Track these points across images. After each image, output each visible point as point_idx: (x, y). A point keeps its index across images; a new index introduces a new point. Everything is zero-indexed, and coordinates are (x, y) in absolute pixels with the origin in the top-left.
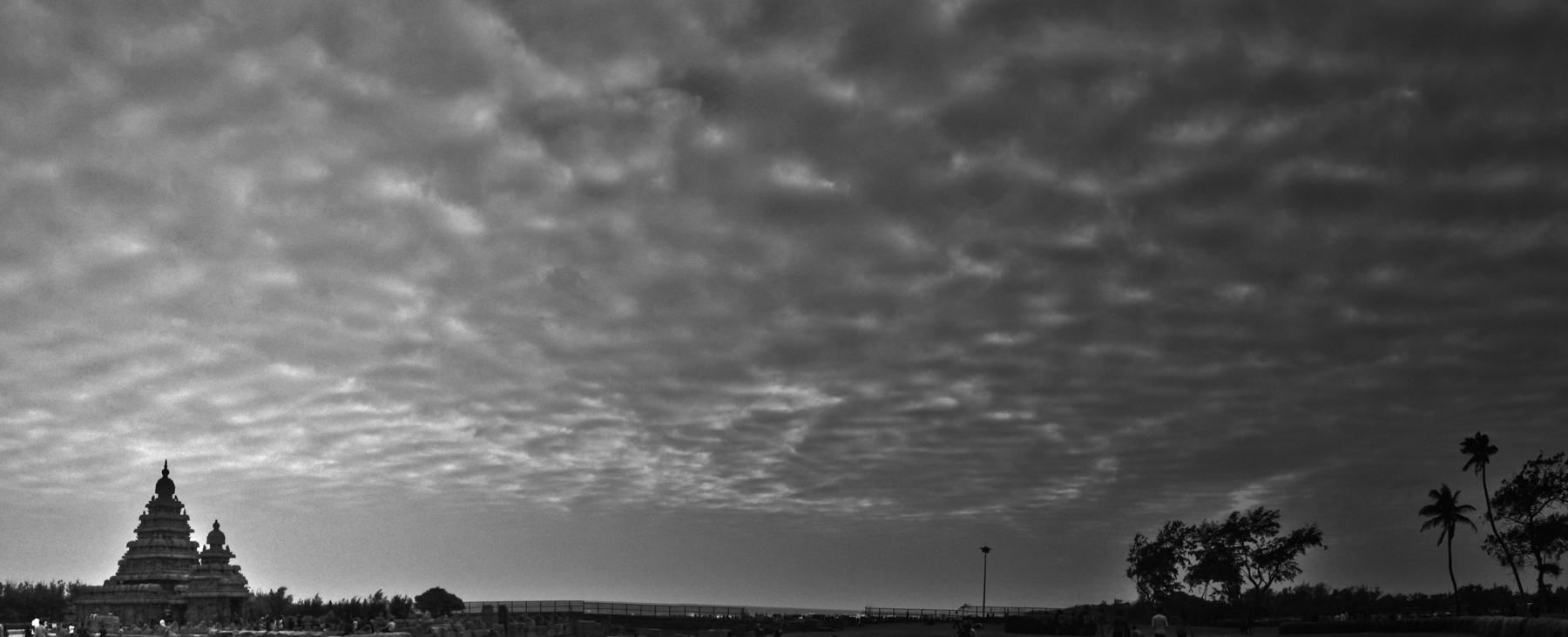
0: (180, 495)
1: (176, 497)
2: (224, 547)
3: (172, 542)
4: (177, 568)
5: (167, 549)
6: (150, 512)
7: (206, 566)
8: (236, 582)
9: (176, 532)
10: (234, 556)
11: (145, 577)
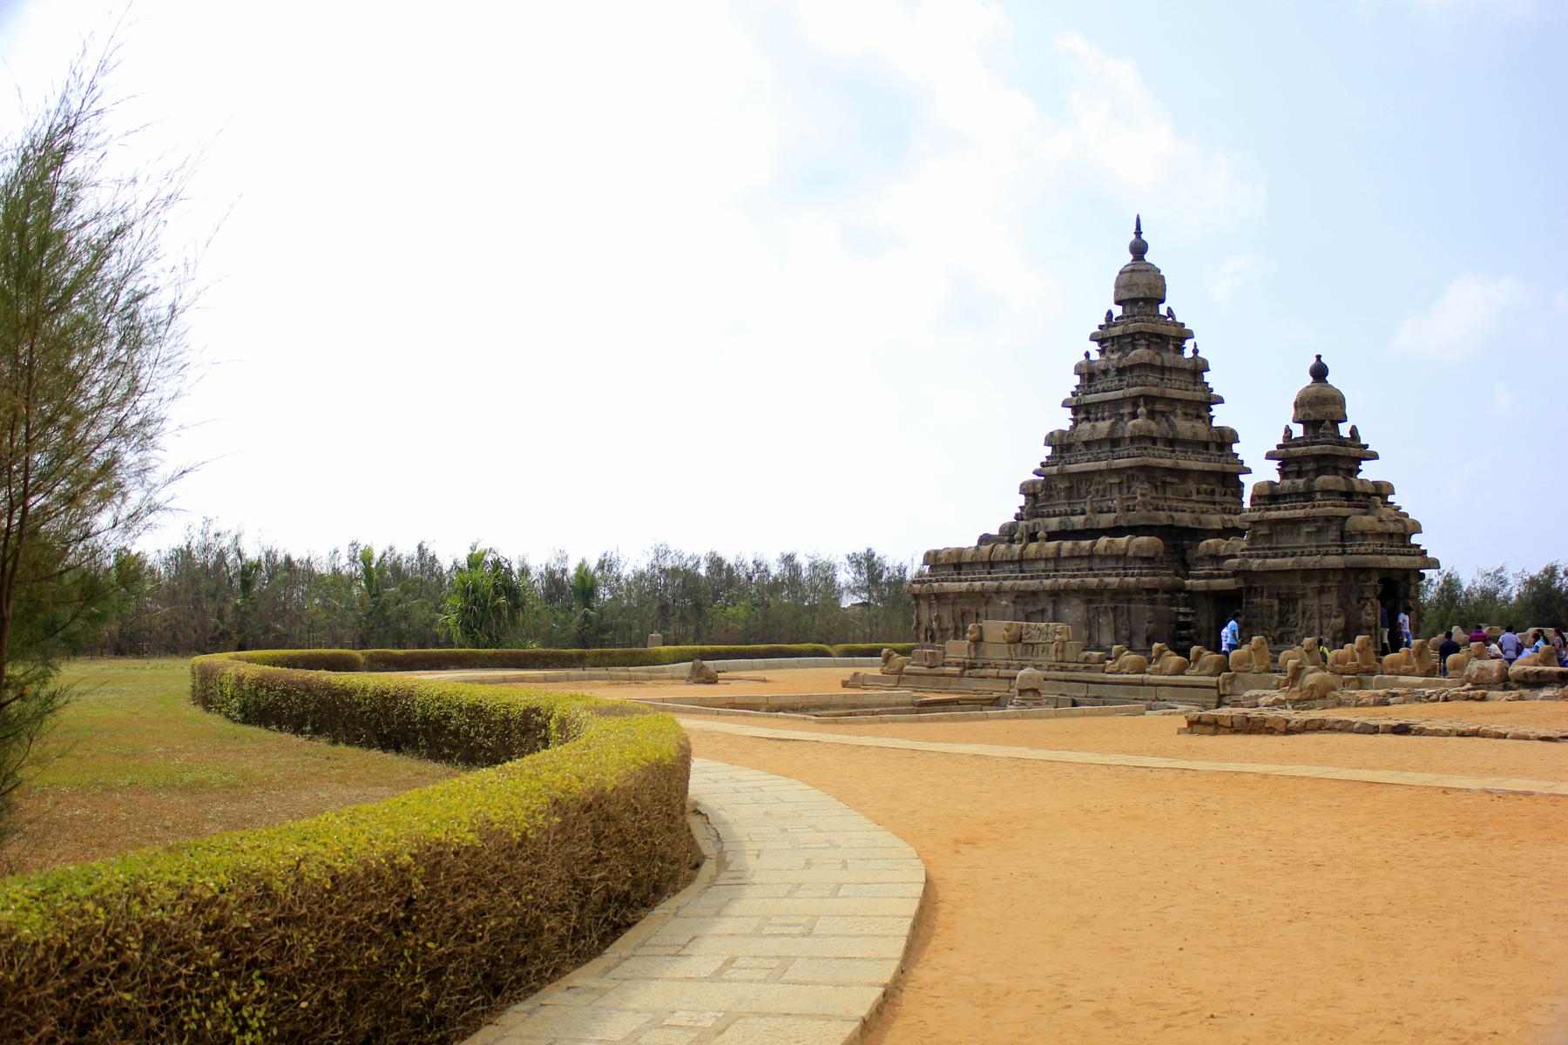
0: (1179, 303)
1: (1169, 308)
2: (1344, 430)
3: (1172, 426)
4: (1187, 497)
5: (1160, 446)
6: (1102, 352)
7: (1300, 482)
8: (1392, 527)
9: (1180, 400)
10: (1374, 456)
11: (1106, 520)
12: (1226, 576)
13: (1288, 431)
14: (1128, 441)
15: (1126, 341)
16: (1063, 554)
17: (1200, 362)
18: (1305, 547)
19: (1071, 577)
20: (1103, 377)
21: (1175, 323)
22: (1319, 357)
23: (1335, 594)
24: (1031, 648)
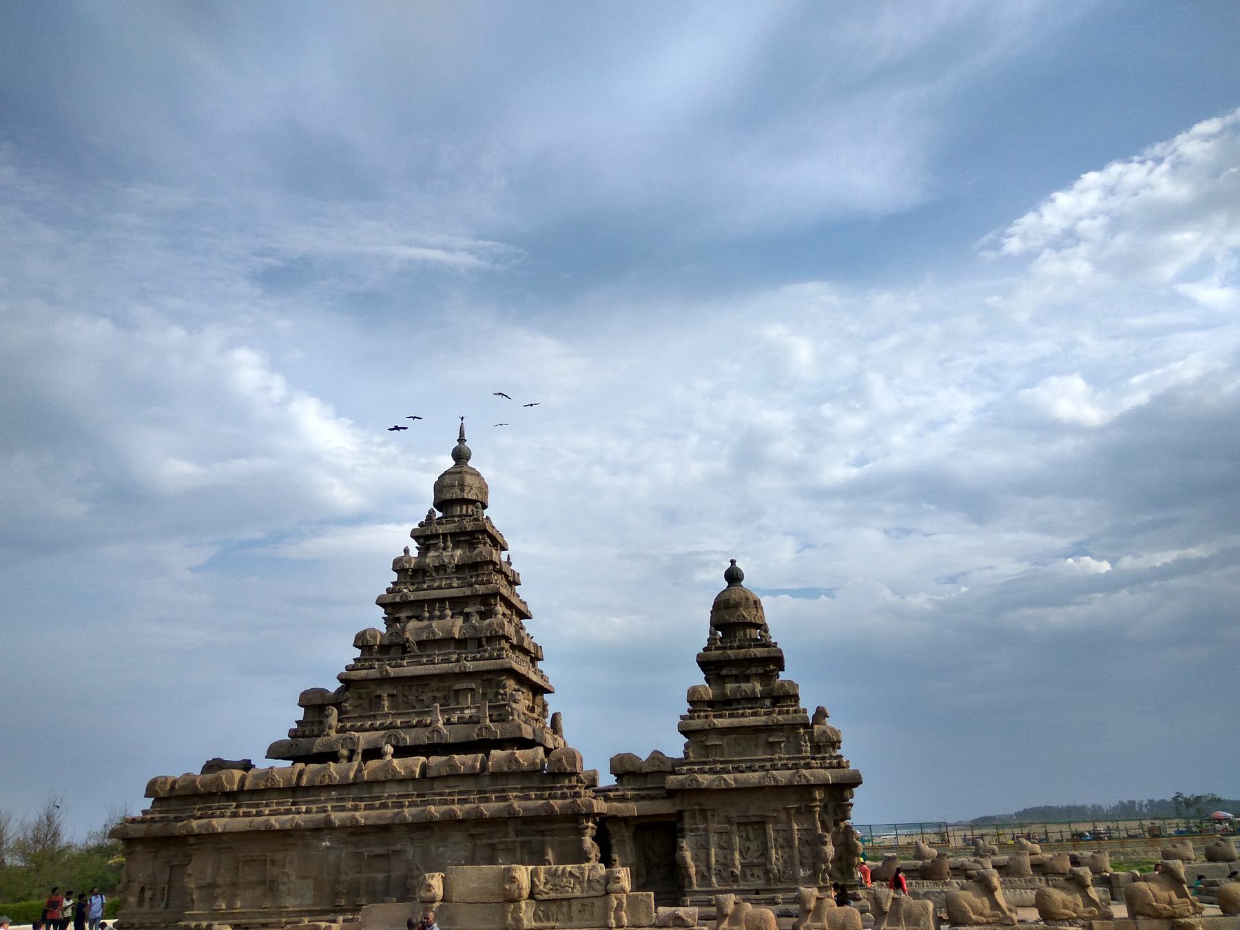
6: (424, 549)
12: (653, 798)
13: (711, 633)
14: (484, 641)
15: (462, 539)
16: (431, 773)
17: (516, 575)
18: (771, 760)
19: (453, 802)
20: (434, 574)
21: (498, 531)
22: (733, 562)
23: (817, 816)
24: (553, 908)
